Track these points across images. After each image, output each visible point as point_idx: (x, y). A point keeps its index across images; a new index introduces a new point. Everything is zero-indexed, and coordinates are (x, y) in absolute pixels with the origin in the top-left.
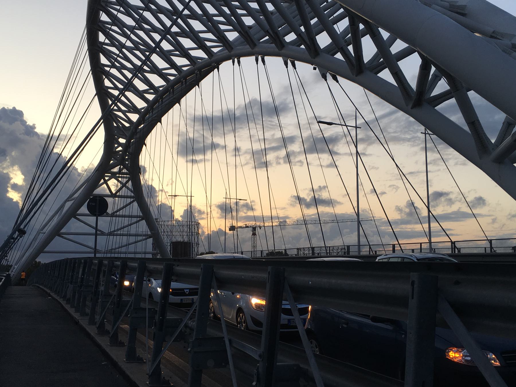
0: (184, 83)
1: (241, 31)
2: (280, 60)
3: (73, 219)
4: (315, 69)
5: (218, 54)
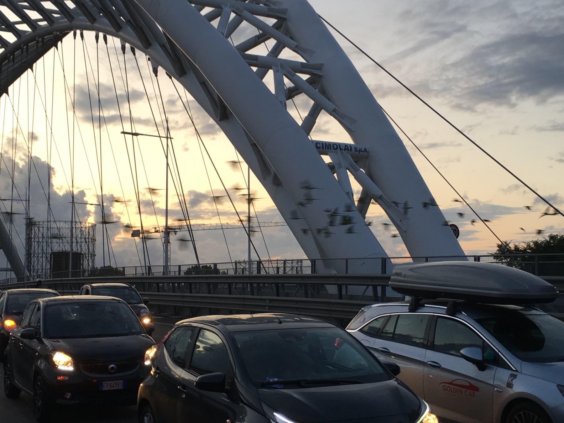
0: (25, 50)
4: (149, 59)
5: (60, 21)
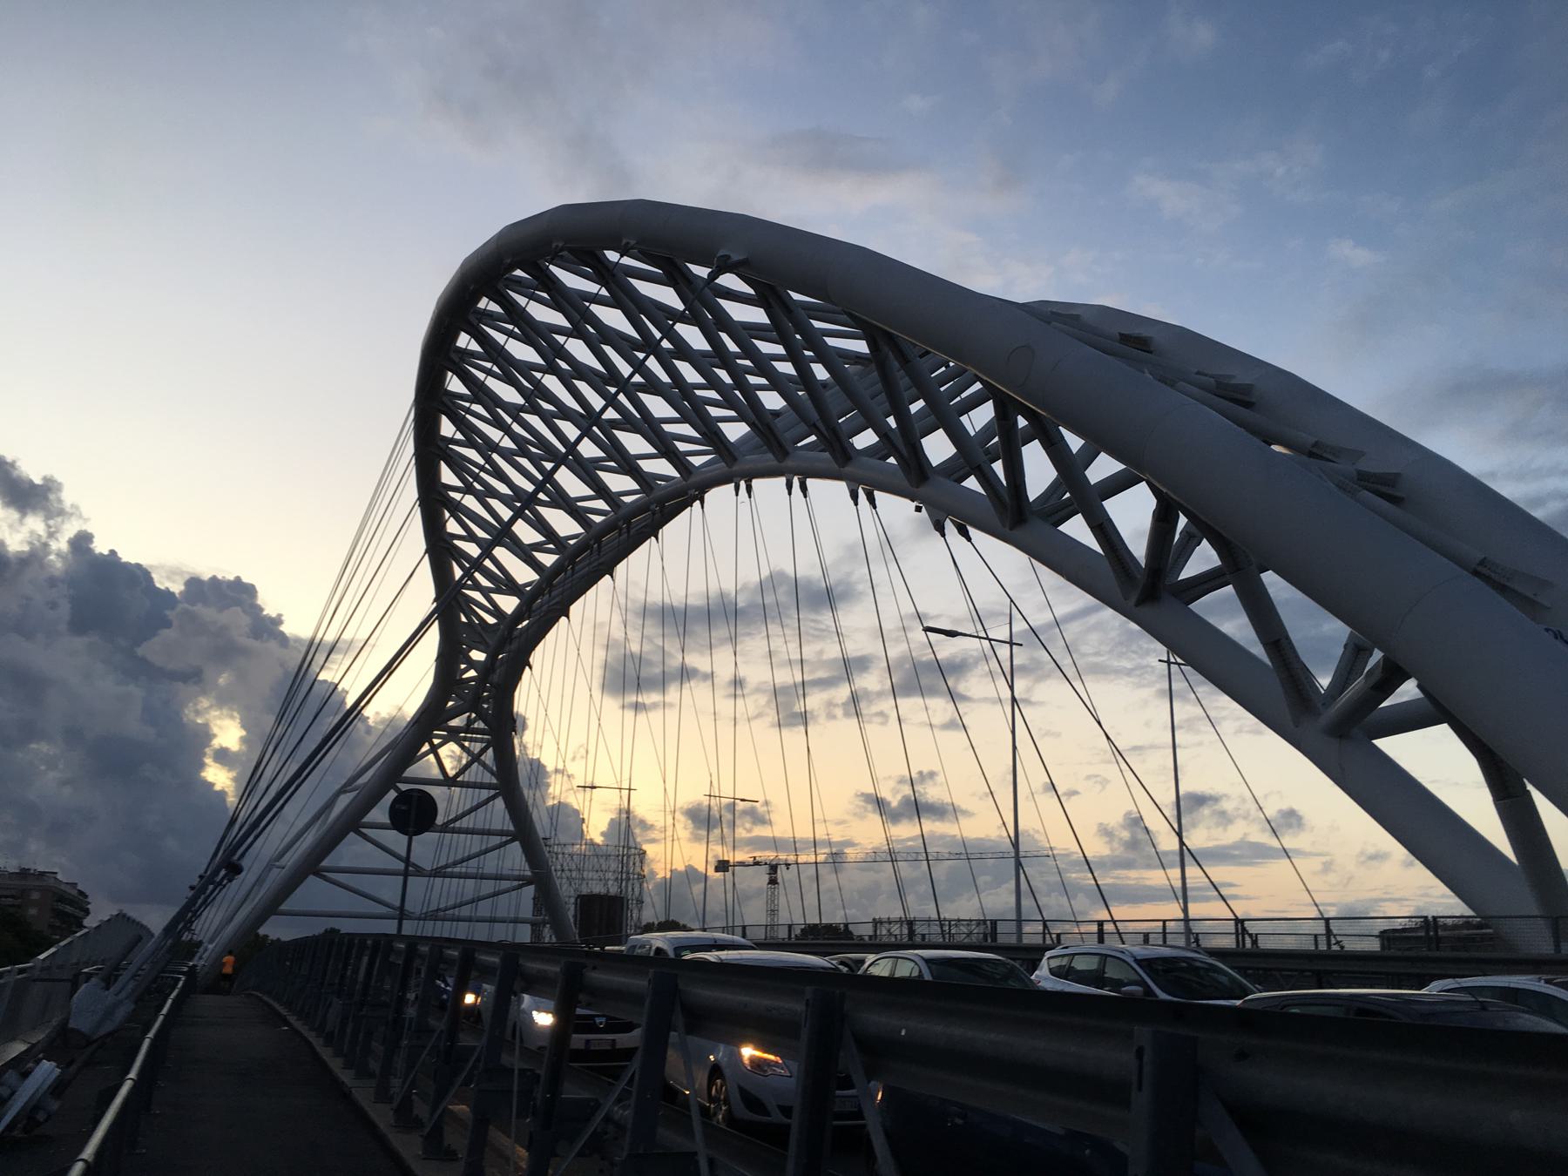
0: (625, 530)
1: (757, 422)
2: (840, 488)
3: (352, 835)
4: (918, 509)
5: (703, 470)
